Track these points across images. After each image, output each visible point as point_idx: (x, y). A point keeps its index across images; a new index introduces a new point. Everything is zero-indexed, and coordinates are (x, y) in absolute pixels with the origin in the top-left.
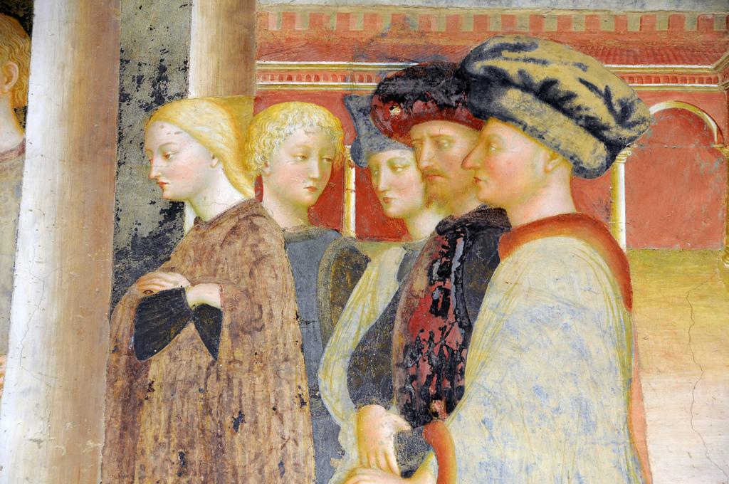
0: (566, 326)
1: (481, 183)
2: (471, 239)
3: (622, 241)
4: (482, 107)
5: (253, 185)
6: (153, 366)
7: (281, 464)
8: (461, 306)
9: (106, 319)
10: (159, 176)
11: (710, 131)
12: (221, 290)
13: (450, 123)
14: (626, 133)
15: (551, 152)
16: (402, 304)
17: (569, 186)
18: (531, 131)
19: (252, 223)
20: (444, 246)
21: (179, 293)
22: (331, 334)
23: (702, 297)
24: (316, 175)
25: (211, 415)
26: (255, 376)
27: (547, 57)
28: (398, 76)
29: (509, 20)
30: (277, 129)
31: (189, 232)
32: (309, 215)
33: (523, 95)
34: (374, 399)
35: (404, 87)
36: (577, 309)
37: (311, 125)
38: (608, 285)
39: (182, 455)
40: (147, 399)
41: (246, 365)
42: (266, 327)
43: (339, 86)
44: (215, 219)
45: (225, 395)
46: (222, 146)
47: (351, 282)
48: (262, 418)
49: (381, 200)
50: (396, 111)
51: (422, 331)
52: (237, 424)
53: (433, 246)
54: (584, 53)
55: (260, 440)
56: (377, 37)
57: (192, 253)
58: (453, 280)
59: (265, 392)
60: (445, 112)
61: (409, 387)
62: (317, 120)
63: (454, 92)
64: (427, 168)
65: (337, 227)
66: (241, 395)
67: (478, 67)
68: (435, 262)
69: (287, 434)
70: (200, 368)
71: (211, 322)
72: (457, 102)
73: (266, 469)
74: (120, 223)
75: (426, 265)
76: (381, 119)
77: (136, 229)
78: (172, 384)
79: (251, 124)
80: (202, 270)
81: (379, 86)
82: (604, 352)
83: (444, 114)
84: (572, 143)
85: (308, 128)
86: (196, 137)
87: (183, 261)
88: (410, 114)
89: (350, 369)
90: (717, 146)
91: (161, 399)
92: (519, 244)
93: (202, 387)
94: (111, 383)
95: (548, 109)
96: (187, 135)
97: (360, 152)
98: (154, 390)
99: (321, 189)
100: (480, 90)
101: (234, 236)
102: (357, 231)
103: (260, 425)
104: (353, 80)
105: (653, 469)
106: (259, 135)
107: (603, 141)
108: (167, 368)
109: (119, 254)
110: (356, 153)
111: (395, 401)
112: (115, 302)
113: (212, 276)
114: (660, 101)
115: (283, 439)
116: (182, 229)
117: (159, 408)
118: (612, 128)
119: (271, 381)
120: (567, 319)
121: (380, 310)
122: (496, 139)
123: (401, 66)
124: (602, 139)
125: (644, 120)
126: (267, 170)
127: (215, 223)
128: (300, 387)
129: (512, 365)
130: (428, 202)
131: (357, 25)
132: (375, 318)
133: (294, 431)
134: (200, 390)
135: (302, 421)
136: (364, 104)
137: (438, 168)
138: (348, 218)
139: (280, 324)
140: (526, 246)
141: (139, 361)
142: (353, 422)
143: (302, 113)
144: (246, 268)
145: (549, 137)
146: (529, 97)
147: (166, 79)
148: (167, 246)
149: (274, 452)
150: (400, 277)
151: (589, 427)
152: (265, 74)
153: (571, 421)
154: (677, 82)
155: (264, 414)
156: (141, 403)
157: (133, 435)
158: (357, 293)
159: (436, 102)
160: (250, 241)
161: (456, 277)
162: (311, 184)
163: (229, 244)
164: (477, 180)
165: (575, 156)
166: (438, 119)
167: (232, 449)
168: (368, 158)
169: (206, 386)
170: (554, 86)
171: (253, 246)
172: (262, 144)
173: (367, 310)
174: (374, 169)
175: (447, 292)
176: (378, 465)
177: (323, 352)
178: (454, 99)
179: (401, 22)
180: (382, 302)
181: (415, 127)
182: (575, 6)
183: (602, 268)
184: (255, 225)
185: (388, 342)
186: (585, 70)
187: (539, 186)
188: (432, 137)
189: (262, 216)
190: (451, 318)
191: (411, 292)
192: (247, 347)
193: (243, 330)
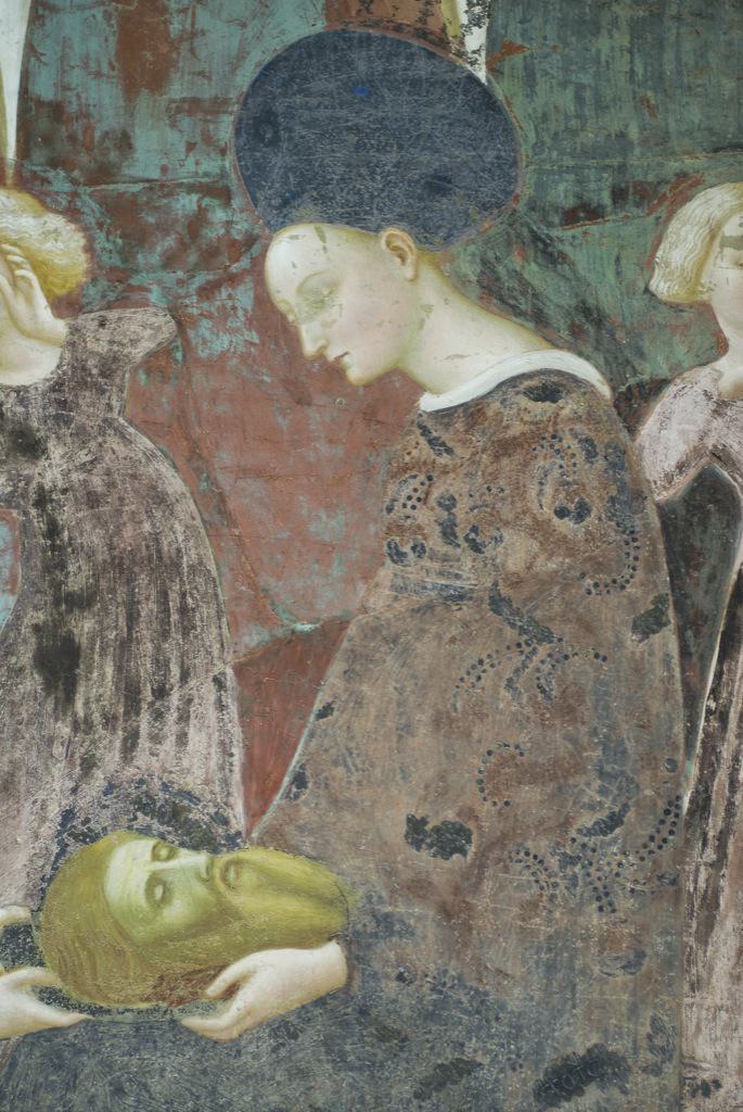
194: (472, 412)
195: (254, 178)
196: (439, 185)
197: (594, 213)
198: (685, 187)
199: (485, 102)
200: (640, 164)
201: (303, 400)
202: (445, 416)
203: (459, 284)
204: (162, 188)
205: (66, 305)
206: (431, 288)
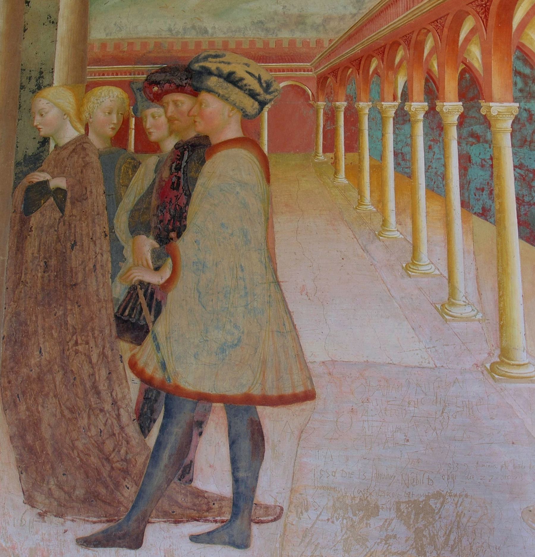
0: (238, 193)
1: (197, 123)
2: (191, 151)
3: (266, 149)
4: (198, 86)
5: (84, 127)
6: (33, 219)
7: (95, 266)
8: (186, 185)
9: (11, 196)
10: (38, 125)
11: (308, 95)
12: (67, 180)
13: (182, 94)
14: (268, 97)
15: (232, 107)
16: (156, 184)
17: (240, 123)
18: (222, 97)
19: (83, 146)
20: (178, 155)
21: (45, 183)
22: (121, 201)
23: (303, 176)
24: (115, 122)
25: (60, 242)
26: (82, 222)
27: (230, 61)
28: (157, 72)
29: (212, 44)
30: (97, 100)
31: (52, 152)
32: (111, 142)
33: (218, 80)
34: (141, 232)
35: (159, 77)
37: (113, 97)
38: (259, 172)
39: (45, 263)
40: (29, 235)
41: (78, 217)
42: (89, 198)
43: (127, 77)
44: (64, 145)
45: (67, 232)
46: (70, 109)
47: (132, 174)
48: (86, 243)
49: (147, 133)
50: (156, 89)
51: (166, 198)
53: (173, 155)
54: (248, 58)
55: (84, 254)
56: (147, 53)
57: (53, 162)
58: (182, 172)
59: (87, 230)
60: (180, 89)
61: (159, 226)
62: (116, 94)
63: (184, 79)
64: (170, 116)
66: (75, 232)
67: (196, 66)
68: (173, 163)
69: (98, 250)
70: (55, 219)
71: (61, 196)
72: (186, 84)
73: (87, 269)
74: (18, 149)
75: (169, 165)
76: (148, 93)
77: (26, 152)
78: (42, 228)
79: (84, 98)
80: (57, 170)
81: (147, 77)
83: (179, 90)
84: (242, 102)
85: (111, 99)
86: (56, 105)
87: (48, 167)
88: (162, 90)
89: (130, 218)
90: (311, 102)
91: (36, 235)
92: (215, 153)
93: (56, 229)
94: (12, 228)
95: (230, 86)
96: (52, 104)
97: (137, 109)
98: (32, 231)
99: (117, 130)
100: (197, 78)
101: (74, 154)
102: (135, 149)
103: (84, 247)
104: (134, 75)
105: (278, 261)
106: (88, 102)
107: (257, 101)
108: (39, 220)
109: (18, 164)
110: (135, 111)
111: (152, 233)
112: (15, 187)
113: (62, 174)
114: (284, 81)
115: (96, 253)
116: (48, 151)
117: (35, 239)
118: (261, 94)
119: (91, 225)
120: (238, 189)
121: (146, 188)
122: (204, 101)
123: (158, 67)
124: (256, 100)
125: (277, 90)
126: (91, 120)
127: (65, 147)
128: (104, 228)
129: (211, 213)
130: (171, 132)
131: (138, 48)
132: (142, 192)
133: (101, 249)
134: (55, 230)
136: (140, 85)
137: (175, 116)
138: (131, 141)
139: (95, 196)
140: (219, 154)
141: (26, 217)
142: (131, 244)
143: (109, 91)
144: (79, 169)
145: (231, 99)
146: (221, 80)
147: (43, 77)
148: (41, 160)
149: (91, 260)
150: (155, 172)
153: (239, 240)
154: (293, 72)
155: (87, 241)
156: (26, 237)
157: (22, 254)
158: (135, 179)
159: (175, 84)
160: (82, 156)
161: (184, 171)
162: (112, 126)
163: (71, 157)
164: (195, 122)
165: (243, 109)
166: (176, 92)
167: (70, 259)
168: (141, 113)
169: (58, 229)
170: (234, 75)
171: (83, 158)
172: (89, 108)
173: (139, 188)
174: (144, 118)
175: (179, 178)
176: (143, 265)
177: (117, 209)
178: (185, 81)
179: (158, 45)
180: (147, 183)
181: (165, 96)
182: (244, 36)
183: (256, 164)
184: (84, 148)
186: (248, 67)
188: (173, 101)
189: (88, 143)
190: (181, 191)
191: (161, 178)
192: (79, 208)
193: (77, 200)
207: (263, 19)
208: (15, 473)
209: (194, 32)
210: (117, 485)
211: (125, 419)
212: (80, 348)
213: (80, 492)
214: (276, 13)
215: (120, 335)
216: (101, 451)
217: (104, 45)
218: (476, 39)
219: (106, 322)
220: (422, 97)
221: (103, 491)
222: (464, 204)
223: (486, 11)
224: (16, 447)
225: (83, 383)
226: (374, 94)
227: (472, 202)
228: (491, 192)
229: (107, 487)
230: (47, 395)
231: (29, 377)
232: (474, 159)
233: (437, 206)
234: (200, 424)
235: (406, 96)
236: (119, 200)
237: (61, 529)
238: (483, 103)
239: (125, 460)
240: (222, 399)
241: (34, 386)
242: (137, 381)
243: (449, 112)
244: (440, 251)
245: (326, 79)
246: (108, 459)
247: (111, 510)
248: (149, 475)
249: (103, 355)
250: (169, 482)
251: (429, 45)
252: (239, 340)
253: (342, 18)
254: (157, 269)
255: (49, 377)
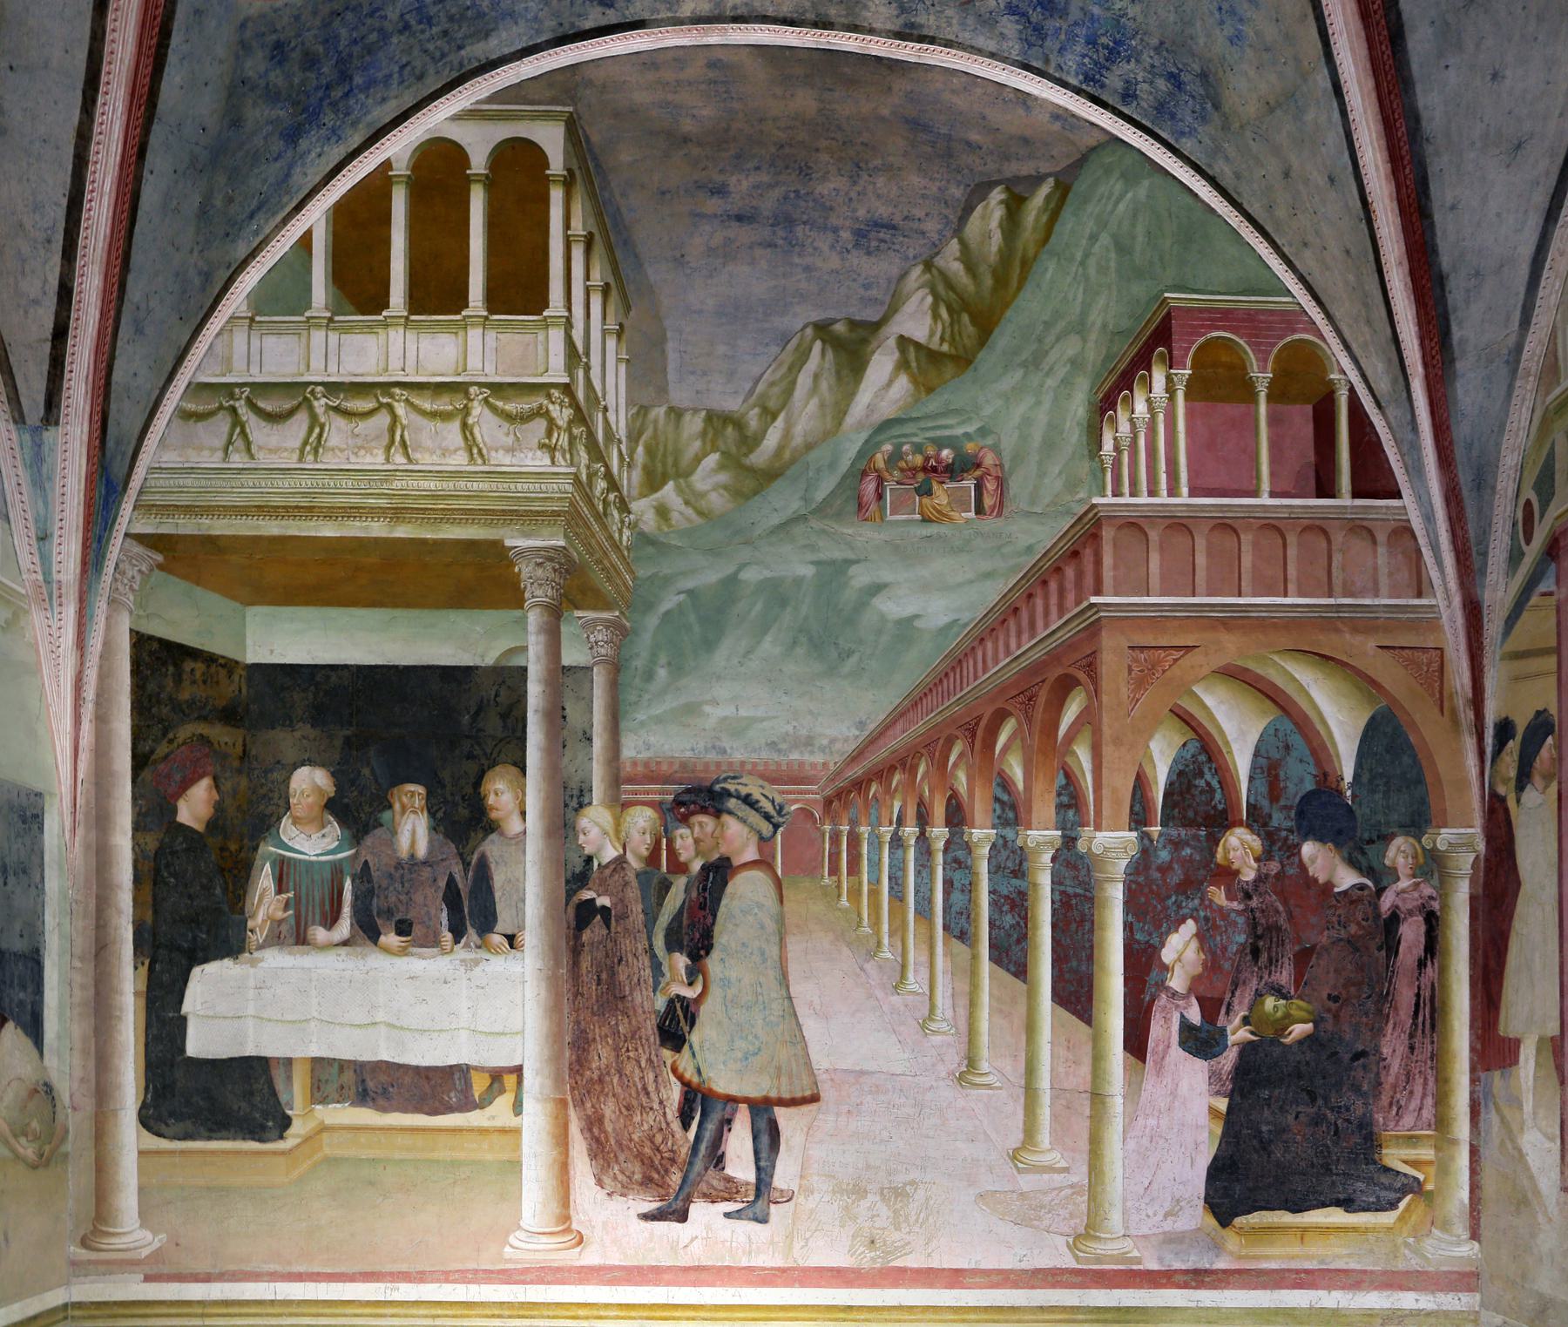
3: (779, 873)
14: (781, 820)
29: (731, 764)
35: (686, 798)
36: (760, 906)
43: (657, 797)
52: (620, 961)
65: (659, 866)
67: (717, 787)
82: (771, 926)
86: (597, 824)
95: (748, 808)
110: (666, 831)
113: (605, 893)
120: (756, 910)
130: (697, 854)
131: (665, 767)
135: (645, 960)
151: (764, 961)
152: (626, 792)
179: (683, 765)
180: (678, 904)
185: (681, 922)
187: (745, 845)
194: (1345, 893)
195: (1299, 828)
196: (1340, 832)
197: (1373, 842)
198: (1393, 836)
199: (1350, 810)
200: (1384, 830)
201: (1309, 887)
202: (1339, 893)
203: (1343, 859)
204: (1279, 829)
205: (1257, 860)
206: (1337, 860)
207: (776, 739)
208: (587, 1159)
209: (714, 752)
210: (667, 1171)
211: (670, 1116)
212: (631, 1054)
213: (638, 1177)
214: (787, 734)
215: (663, 1044)
216: (652, 1142)
217: (635, 764)
218: (963, 766)
219: (650, 1032)
220: (914, 822)
221: (656, 1176)
222: (946, 928)
223: (974, 736)
224: (585, 1139)
225: (635, 1085)
226: (873, 818)
227: (953, 925)
228: (968, 917)
229: (659, 1173)
230: (607, 1095)
231: (592, 1079)
232: (957, 885)
233: (923, 929)
234: (729, 1121)
235: (901, 821)
236: (655, 919)
237: (625, 1207)
238: (965, 828)
239: (672, 1151)
240: (746, 1100)
241: (596, 1087)
242: (679, 1083)
243: (937, 838)
244: (924, 973)
245: (831, 802)
246: (658, 1150)
247: (662, 1192)
248: (691, 1164)
249: (649, 1060)
250: (706, 1169)
251: (921, 769)
252: (759, 1050)
253: (846, 740)
254: (690, 984)
255: (607, 1079)
